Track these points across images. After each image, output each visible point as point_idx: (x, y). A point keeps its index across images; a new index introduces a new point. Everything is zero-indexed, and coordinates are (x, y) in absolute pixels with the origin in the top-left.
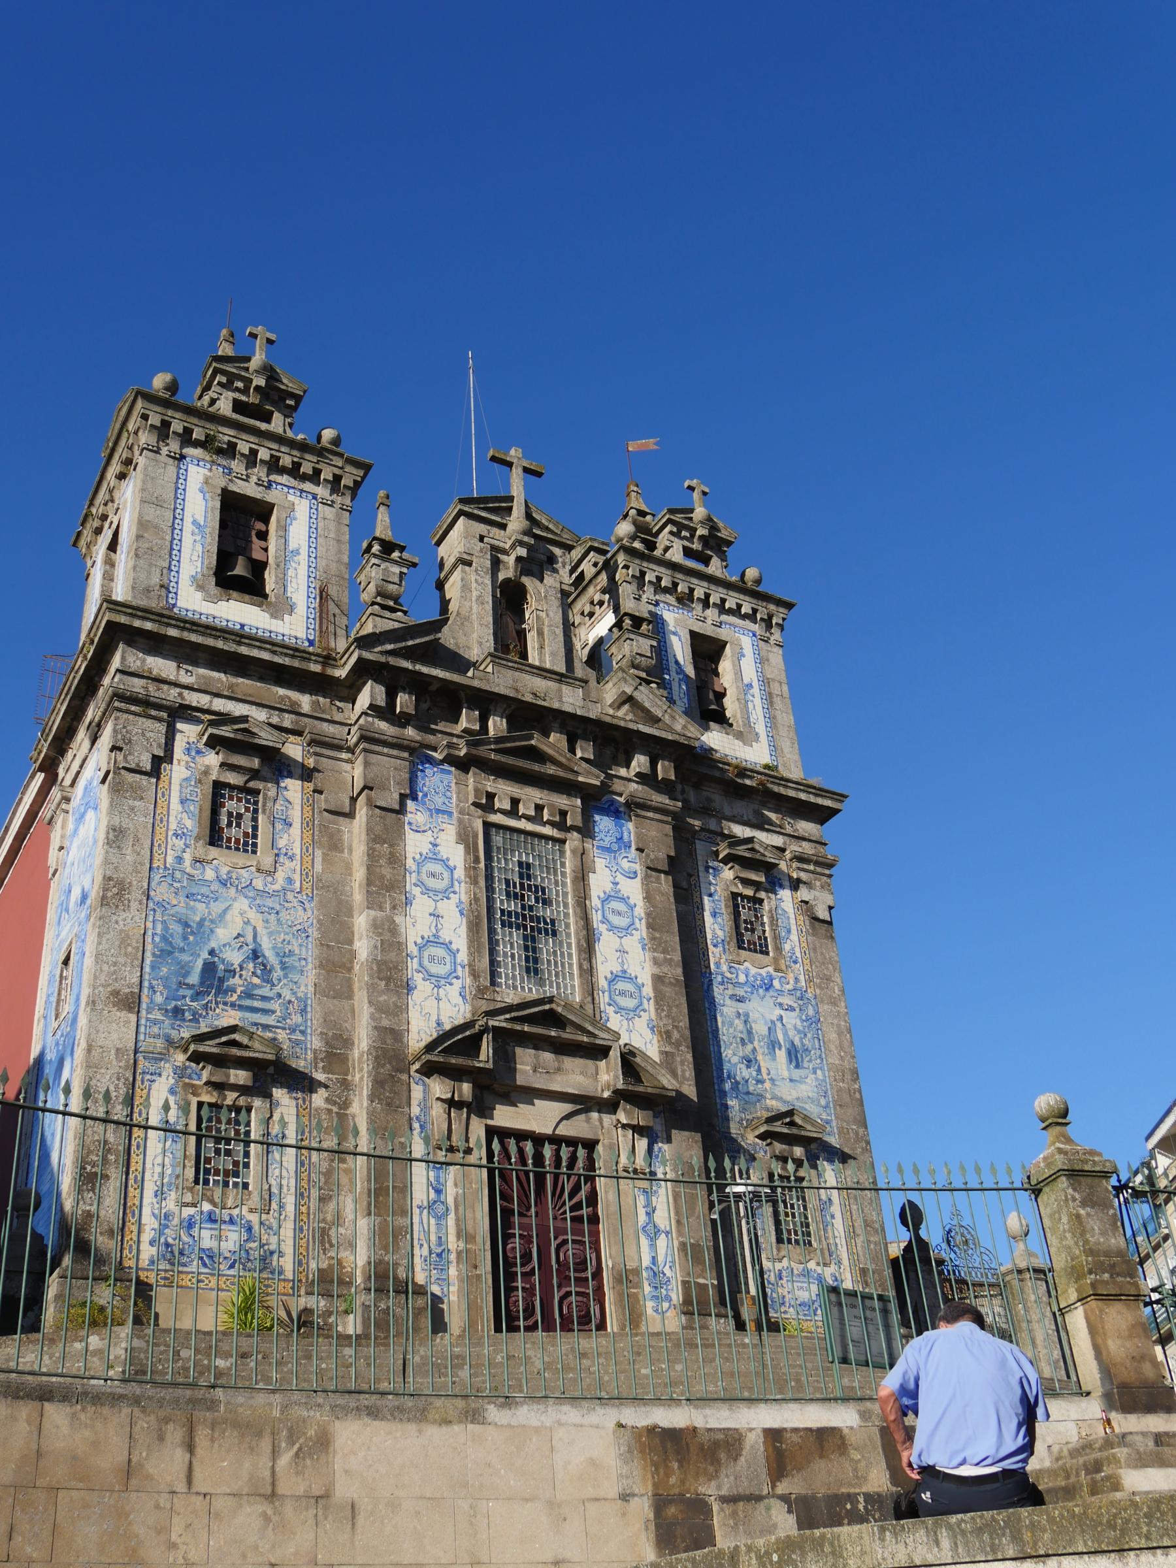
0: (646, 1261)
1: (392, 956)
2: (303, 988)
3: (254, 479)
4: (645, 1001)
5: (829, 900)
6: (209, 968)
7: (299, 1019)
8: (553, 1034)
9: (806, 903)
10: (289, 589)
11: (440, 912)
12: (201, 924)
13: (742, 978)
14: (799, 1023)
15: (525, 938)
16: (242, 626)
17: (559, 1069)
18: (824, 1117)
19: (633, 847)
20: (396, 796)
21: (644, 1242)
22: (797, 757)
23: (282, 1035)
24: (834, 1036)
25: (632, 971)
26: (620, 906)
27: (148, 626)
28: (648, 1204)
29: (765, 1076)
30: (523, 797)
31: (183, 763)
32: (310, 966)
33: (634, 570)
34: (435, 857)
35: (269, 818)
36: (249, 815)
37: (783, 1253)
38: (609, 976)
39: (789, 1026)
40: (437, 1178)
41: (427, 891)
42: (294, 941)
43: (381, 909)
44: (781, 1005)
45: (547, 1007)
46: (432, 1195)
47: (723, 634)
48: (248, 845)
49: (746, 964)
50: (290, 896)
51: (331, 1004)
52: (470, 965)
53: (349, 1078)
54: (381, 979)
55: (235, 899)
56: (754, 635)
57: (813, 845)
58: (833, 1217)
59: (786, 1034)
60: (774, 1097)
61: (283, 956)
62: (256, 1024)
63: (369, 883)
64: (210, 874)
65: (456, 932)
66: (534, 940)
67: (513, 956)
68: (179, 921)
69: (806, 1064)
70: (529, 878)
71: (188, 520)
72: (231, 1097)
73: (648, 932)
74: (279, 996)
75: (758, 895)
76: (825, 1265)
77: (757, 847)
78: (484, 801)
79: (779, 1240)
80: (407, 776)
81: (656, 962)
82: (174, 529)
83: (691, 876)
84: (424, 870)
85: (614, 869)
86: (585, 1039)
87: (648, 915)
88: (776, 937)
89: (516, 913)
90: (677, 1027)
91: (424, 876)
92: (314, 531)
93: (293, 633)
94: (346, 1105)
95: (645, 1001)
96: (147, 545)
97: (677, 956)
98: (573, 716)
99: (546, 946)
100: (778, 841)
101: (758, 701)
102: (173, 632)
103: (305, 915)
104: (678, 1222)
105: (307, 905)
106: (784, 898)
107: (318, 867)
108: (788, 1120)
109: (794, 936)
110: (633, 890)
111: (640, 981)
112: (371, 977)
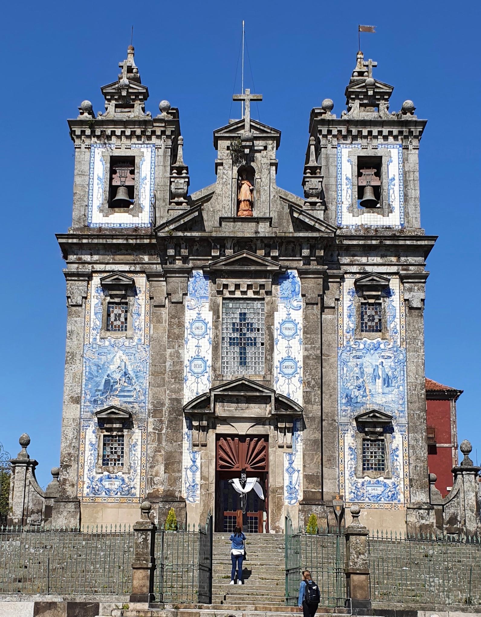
0: (286, 483)
1: (178, 368)
2: (145, 385)
3: (123, 147)
4: (299, 369)
5: (422, 296)
6: (107, 382)
7: (142, 398)
8: (242, 394)
9: (408, 300)
10: (142, 199)
11: (200, 344)
12: (104, 365)
13: (362, 346)
14: (392, 364)
15: (241, 349)
16: (120, 225)
17: (248, 408)
18: (401, 409)
19: (300, 295)
20: (181, 295)
21: (286, 475)
22: (418, 215)
23: (136, 405)
24: (412, 368)
25: (293, 356)
26: (290, 325)
27: (75, 241)
28: (291, 459)
29: (368, 393)
30: (241, 283)
31: (95, 297)
32: (148, 375)
33: (325, 132)
34: (199, 320)
35: (131, 314)
36: (123, 315)
37: (365, 474)
38: (281, 360)
39: (386, 367)
40: (194, 457)
41: (194, 335)
42: (141, 366)
43: (174, 348)
44: (383, 356)
45: (240, 382)
46: (192, 463)
47: (379, 152)
48: (123, 328)
49: (365, 339)
50: (139, 346)
51: (155, 389)
52: (212, 366)
53: (163, 419)
54: (172, 379)
55: (117, 352)
56: (400, 146)
57: (416, 267)
58: (397, 456)
59: (384, 371)
60: (373, 403)
61: (136, 373)
62: (126, 402)
63: (169, 337)
64: (107, 343)
65: (207, 352)
66: (245, 349)
67: (234, 358)
68: (95, 365)
69: (393, 385)
70: (245, 320)
71: (96, 177)
72: (115, 433)
73: (303, 336)
74: (135, 389)
75: (377, 301)
76: (389, 478)
77: (375, 278)
78: (221, 289)
79: (364, 469)
80: (186, 284)
81: (306, 349)
82: (89, 185)
83: (338, 300)
84: (194, 327)
85: (288, 308)
86: (258, 394)
87: (304, 327)
88: (386, 322)
89: (237, 338)
90: (314, 379)
91: (194, 330)
92: (154, 165)
93: (143, 222)
94: (161, 430)
95: (299, 369)
96: (79, 197)
97: (318, 345)
98: (265, 237)
99: (250, 351)
100: (394, 269)
101: (396, 188)
102: (85, 241)
103: (145, 354)
104: (304, 466)
105: (147, 349)
106: (394, 300)
107: (152, 332)
108: (371, 415)
109: (397, 320)
110: (298, 316)
111: (297, 360)
112: (169, 378)
